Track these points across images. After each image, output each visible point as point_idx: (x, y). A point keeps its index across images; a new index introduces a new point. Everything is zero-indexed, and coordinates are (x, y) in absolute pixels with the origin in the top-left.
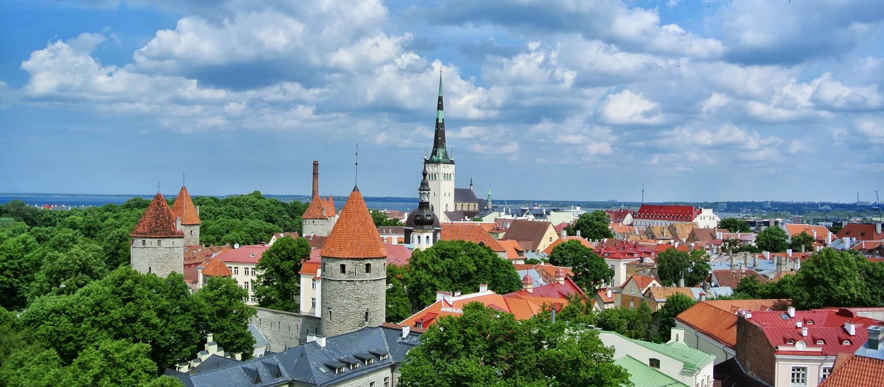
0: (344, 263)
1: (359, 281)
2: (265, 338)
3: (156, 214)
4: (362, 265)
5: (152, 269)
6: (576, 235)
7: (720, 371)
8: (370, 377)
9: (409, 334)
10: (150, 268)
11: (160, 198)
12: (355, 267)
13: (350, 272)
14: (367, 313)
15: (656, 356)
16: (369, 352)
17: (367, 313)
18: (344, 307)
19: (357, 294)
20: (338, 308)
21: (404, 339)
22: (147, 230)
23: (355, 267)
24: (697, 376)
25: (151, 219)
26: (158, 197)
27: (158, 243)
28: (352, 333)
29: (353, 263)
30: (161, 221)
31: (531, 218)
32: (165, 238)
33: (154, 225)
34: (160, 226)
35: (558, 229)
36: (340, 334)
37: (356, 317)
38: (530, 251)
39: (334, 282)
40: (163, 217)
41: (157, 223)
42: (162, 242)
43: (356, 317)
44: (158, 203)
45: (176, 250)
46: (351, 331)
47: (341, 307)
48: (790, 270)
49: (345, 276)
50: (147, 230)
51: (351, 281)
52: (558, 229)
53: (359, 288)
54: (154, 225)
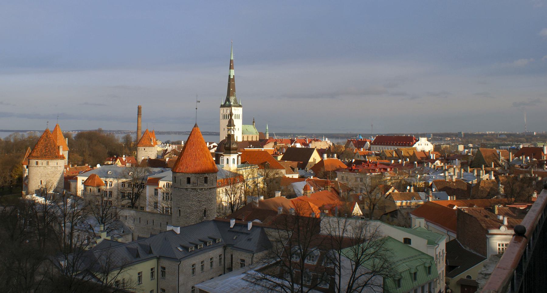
0: (190, 177)
1: (199, 189)
2: (129, 229)
3: (46, 143)
4: (202, 178)
5: (42, 182)
6: (333, 157)
7: (449, 245)
8: (210, 254)
9: (236, 225)
10: (41, 181)
11: (48, 132)
12: (197, 179)
13: (194, 183)
14: (205, 211)
15: (408, 236)
16: (208, 237)
17: (205, 211)
18: (190, 207)
19: (198, 198)
20: (185, 207)
21: (231, 228)
22: (39, 154)
23: (197, 179)
24: (437, 249)
25: (43, 147)
26: (46, 132)
27: (47, 163)
28: (195, 224)
29: (195, 176)
30: (49, 148)
31: (298, 146)
32: (52, 159)
33: (44, 151)
34: (48, 151)
35: (321, 152)
36: (187, 225)
37: (198, 214)
38: (301, 169)
39: (182, 190)
40: (50, 146)
41: (46, 150)
42: (49, 163)
43: (198, 214)
44: (47, 136)
45: (59, 168)
46: (194, 223)
47: (187, 207)
48: (486, 179)
49: (190, 186)
50: (39, 154)
51: (194, 189)
52: (321, 152)
53: (200, 194)
54: (44, 151)
